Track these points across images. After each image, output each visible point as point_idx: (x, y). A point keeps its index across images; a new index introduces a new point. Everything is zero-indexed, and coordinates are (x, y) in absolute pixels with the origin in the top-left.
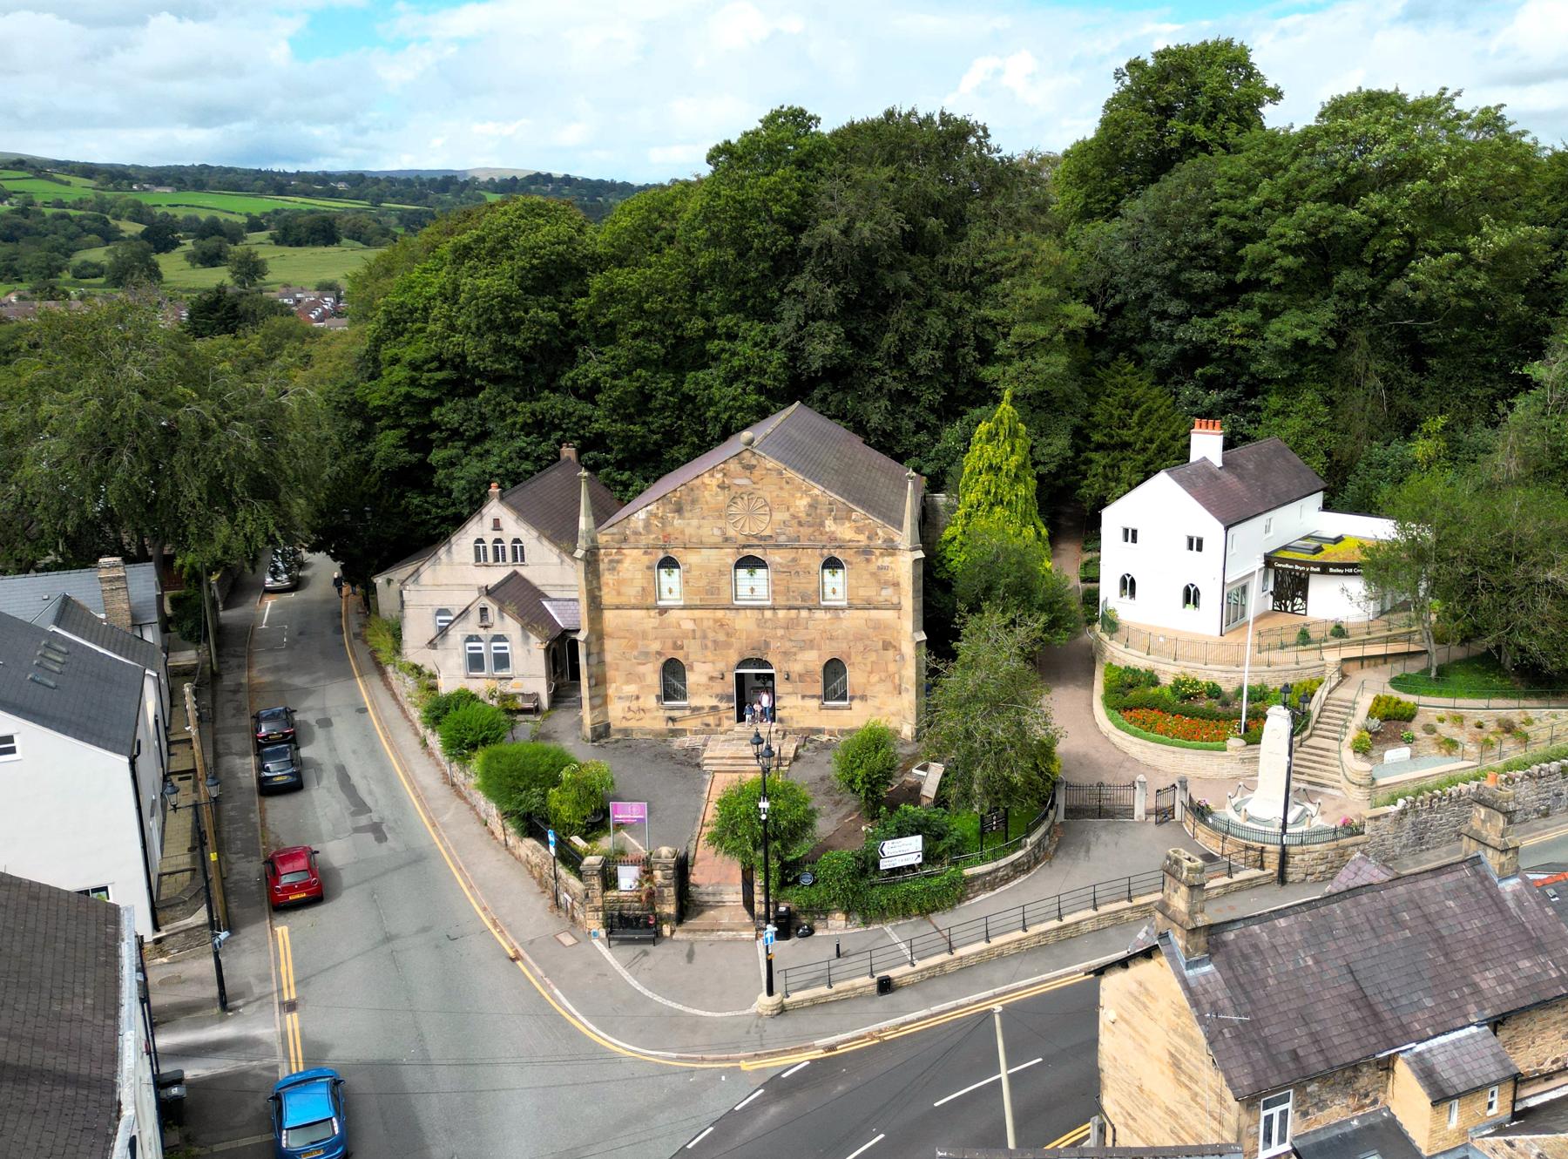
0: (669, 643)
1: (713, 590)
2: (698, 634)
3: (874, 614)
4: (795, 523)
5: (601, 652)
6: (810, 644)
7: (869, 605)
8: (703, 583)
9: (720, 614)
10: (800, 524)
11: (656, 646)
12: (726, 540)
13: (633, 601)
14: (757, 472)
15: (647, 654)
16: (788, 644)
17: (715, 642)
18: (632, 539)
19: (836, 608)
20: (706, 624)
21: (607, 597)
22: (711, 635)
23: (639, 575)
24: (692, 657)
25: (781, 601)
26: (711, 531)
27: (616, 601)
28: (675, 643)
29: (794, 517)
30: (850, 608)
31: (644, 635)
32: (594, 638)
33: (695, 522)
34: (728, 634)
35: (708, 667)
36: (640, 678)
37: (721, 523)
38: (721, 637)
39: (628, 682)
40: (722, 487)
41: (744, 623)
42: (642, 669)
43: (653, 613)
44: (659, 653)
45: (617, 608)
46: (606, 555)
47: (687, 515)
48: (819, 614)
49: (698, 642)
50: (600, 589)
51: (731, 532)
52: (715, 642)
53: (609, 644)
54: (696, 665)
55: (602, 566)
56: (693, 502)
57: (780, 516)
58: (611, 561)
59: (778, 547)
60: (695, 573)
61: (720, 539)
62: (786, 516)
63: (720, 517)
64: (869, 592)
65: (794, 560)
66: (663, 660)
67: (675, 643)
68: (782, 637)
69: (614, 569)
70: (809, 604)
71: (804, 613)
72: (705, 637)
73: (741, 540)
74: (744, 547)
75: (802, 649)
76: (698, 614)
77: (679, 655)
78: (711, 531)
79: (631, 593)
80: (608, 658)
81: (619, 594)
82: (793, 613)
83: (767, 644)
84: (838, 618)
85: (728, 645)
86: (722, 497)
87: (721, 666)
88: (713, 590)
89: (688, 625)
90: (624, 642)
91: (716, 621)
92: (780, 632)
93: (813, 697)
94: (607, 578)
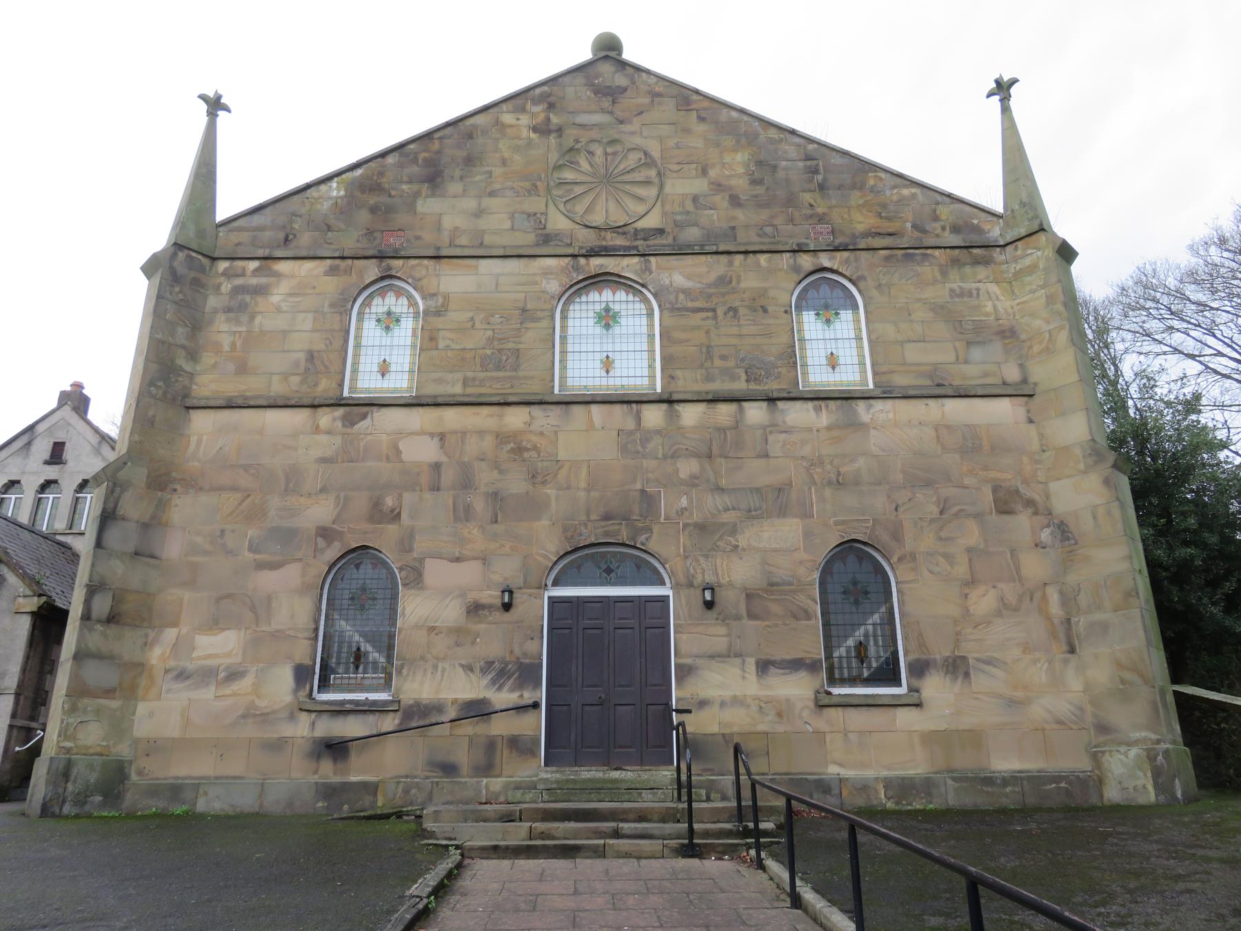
0: (361, 503)
1: (503, 357)
2: (448, 477)
3: (955, 409)
4: (721, 201)
5: (152, 525)
6: (777, 501)
7: (940, 391)
8: (476, 340)
9: (515, 418)
10: (735, 201)
11: (320, 512)
12: (547, 239)
13: (277, 388)
14: (629, 101)
15: (287, 536)
16: (712, 502)
17: (495, 497)
18: (305, 240)
19: (846, 397)
20: (472, 447)
21: (210, 381)
22: (485, 477)
23: (306, 322)
24: (421, 545)
25: (689, 382)
26: (498, 222)
27: (231, 387)
28: (377, 504)
29: (718, 187)
30: (886, 393)
31: (292, 481)
32: (138, 475)
33: (470, 204)
34: (533, 476)
35: (468, 574)
36: (259, 608)
37: (535, 204)
38: (516, 484)
39: (215, 624)
40: (543, 129)
41: (583, 442)
42: (268, 580)
43: (326, 418)
44: (325, 533)
45: (230, 406)
46: (227, 274)
47: (455, 187)
48: (797, 414)
49: (446, 498)
50: (193, 356)
51: (558, 222)
52: (495, 497)
53: (184, 509)
54: (435, 571)
55: (213, 302)
56: (469, 161)
57: (682, 187)
58: (237, 290)
59: (681, 251)
60: (456, 316)
61: (525, 239)
62: (700, 186)
63: (533, 191)
64: (938, 353)
65: (723, 281)
66: (333, 553)
67: (377, 504)
68: (693, 482)
69: (243, 307)
70: (773, 386)
71: (755, 413)
72: (466, 483)
73: (586, 238)
74: (591, 253)
75: (752, 515)
76: (452, 418)
77: (386, 539)
78: (498, 222)
79: (274, 370)
80: (173, 548)
81: (242, 369)
82: (725, 409)
83: (648, 500)
84: (855, 425)
85: (531, 507)
86: (548, 150)
87: (507, 569)
88: (503, 357)
89: (421, 452)
90: (230, 500)
91: (502, 438)
92: (687, 468)
93: (795, 665)
94: (223, 331)
